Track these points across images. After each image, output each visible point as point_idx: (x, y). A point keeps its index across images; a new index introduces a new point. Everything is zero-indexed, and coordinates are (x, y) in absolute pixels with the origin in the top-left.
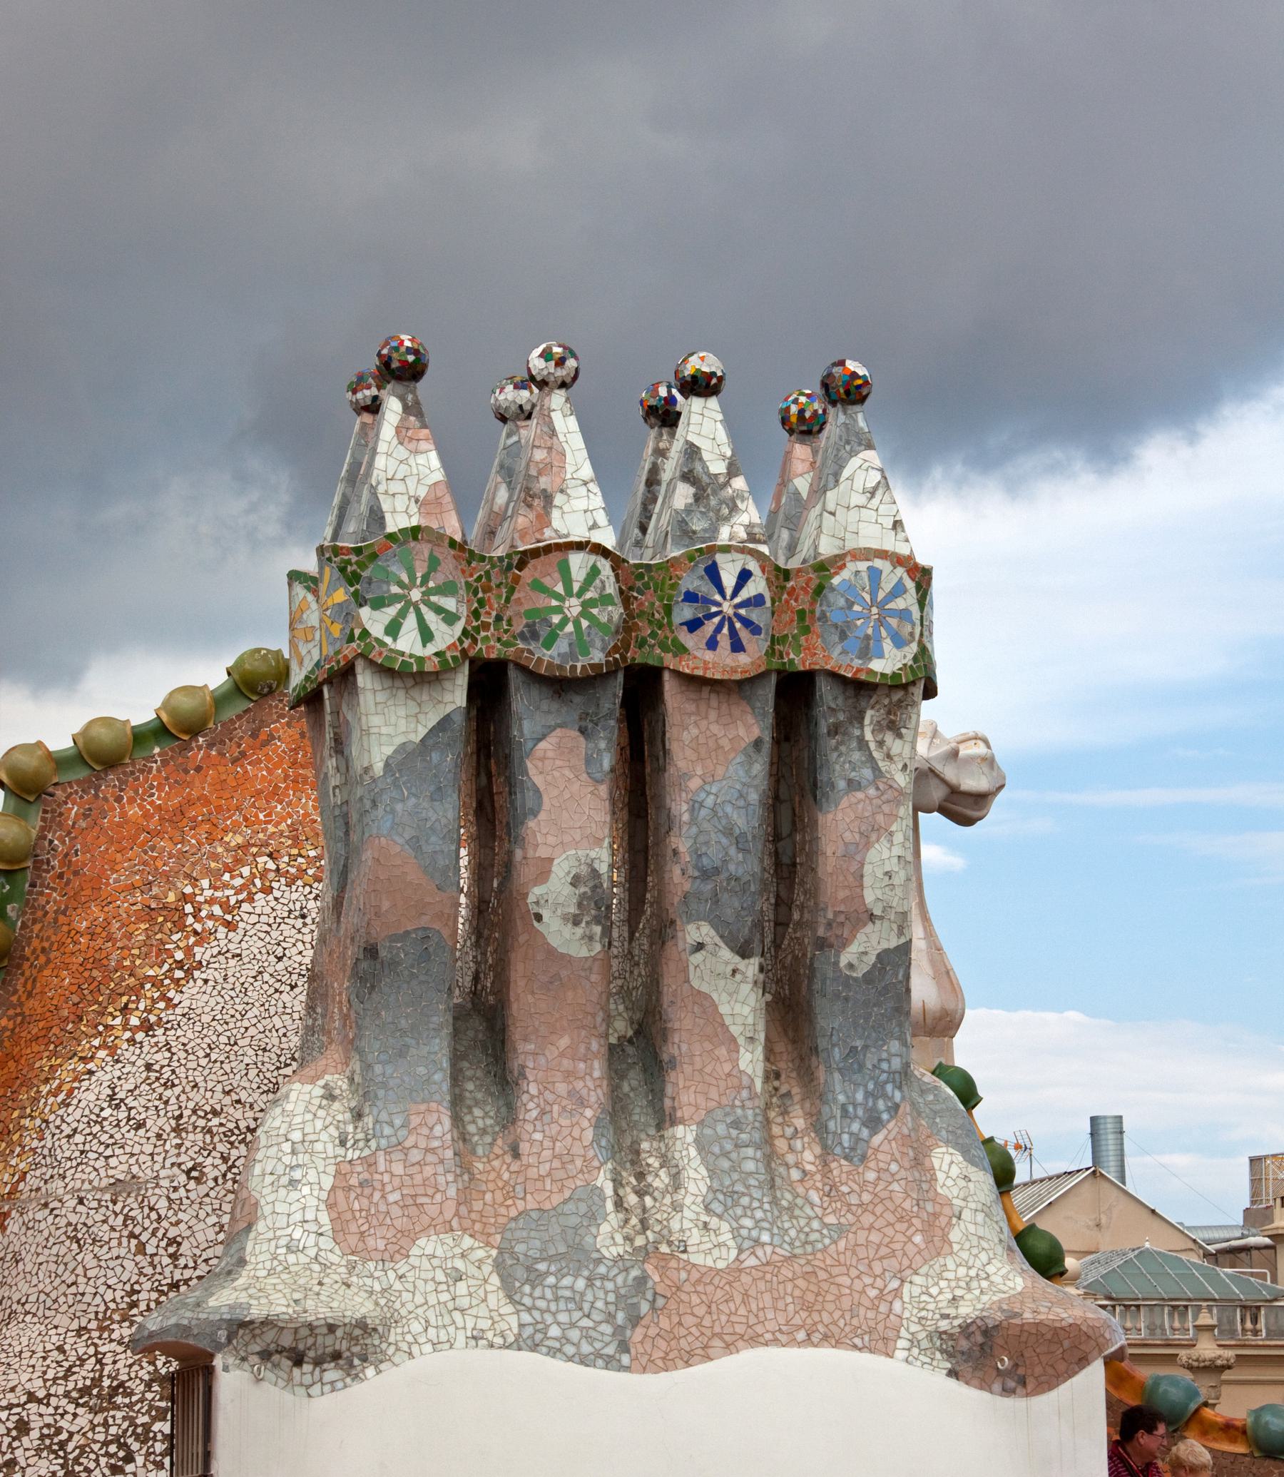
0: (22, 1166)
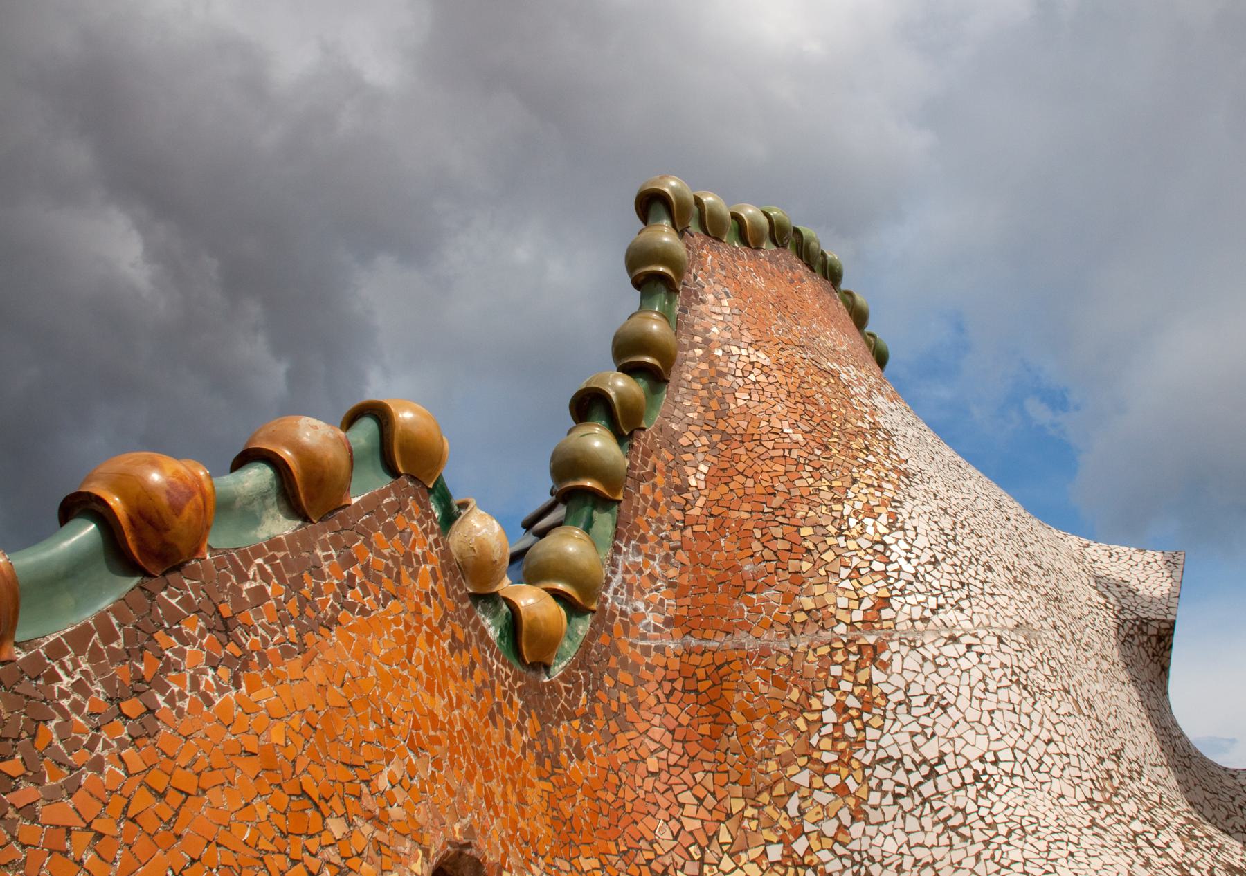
0: (871, 590)
